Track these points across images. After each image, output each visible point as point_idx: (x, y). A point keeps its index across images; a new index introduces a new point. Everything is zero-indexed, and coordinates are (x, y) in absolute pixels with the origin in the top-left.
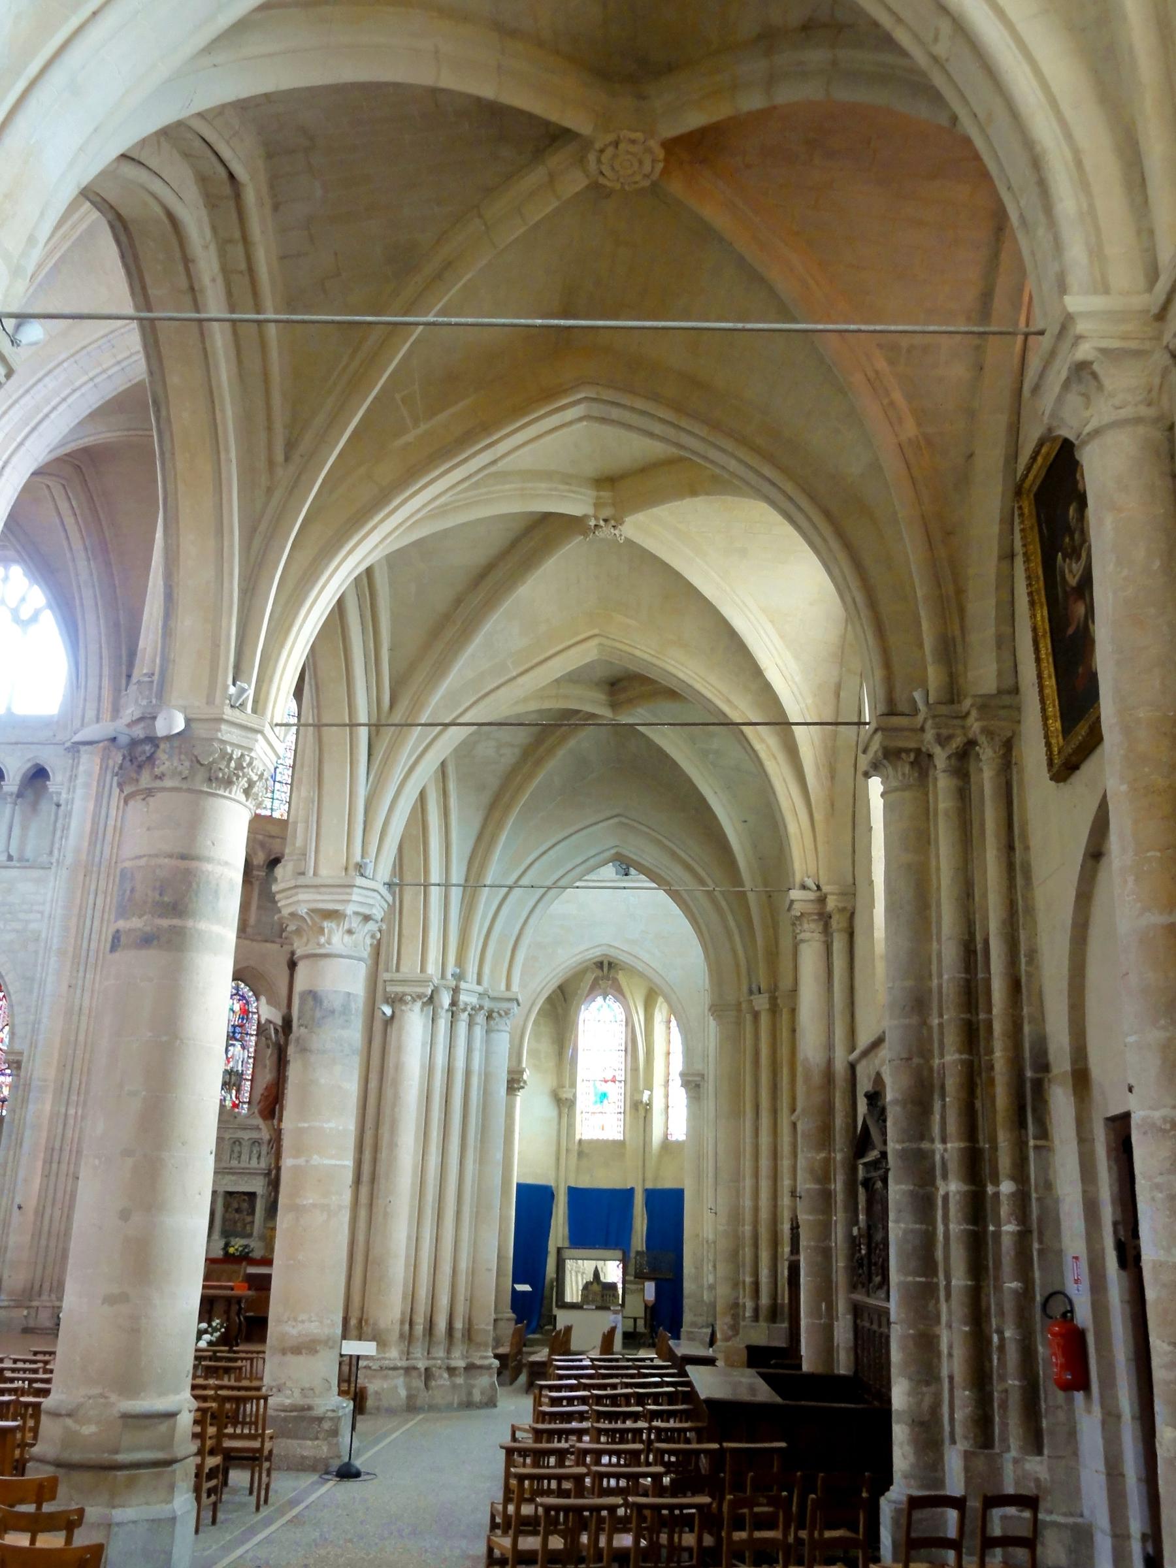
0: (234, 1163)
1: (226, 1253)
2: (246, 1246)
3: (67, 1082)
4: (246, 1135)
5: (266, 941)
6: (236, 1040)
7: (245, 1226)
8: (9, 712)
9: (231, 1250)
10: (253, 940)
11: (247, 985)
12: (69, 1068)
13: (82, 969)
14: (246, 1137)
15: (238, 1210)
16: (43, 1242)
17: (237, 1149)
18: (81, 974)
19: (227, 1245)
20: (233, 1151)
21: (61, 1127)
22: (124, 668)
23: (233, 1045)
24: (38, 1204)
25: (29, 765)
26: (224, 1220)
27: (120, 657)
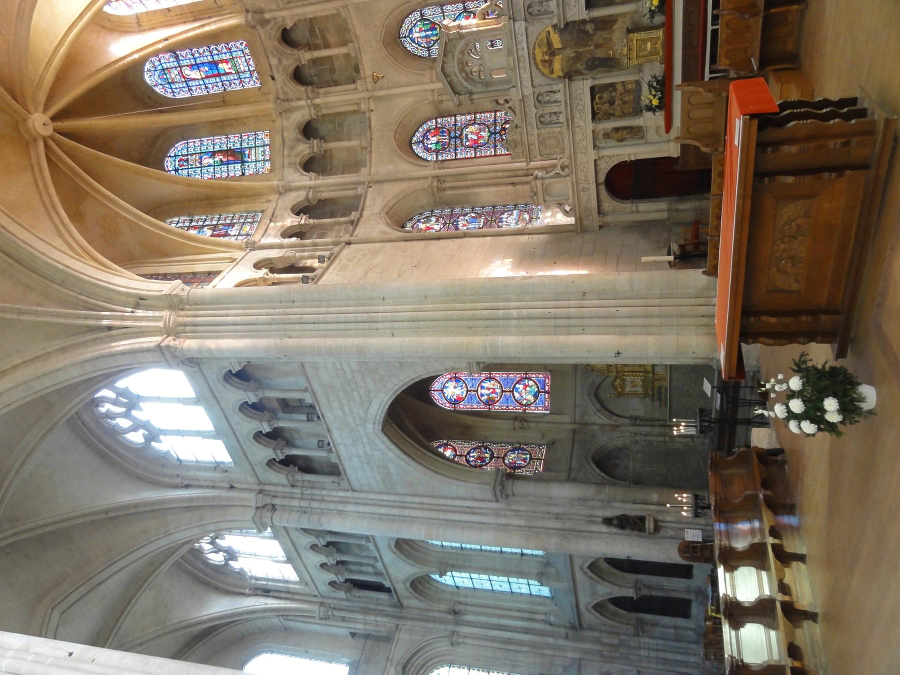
0: (562, 118)
1: (659, 107)
2: (650, 86)
3: (486, 323)
4: (532, 111)
5: (370, 127)
6: (461, 135)
7: (627, 91)
8: (197, 401)
9: (655, 102)
10: (371, 139)
11: (414, 135)
12: (471, 323)
13: (374, 325)
14: (534, 111)
15: (612, 103)
16: (656, 321)
17: (547, 119)
18: (380, 325)
19: (650, 108)
20: (550, 123)
21: (532, 322)
22: (102, 335)
23: (466, 135)
24: (614, 334)
25: (228, 386)
26: (624, 115)
27: (94, 340)
